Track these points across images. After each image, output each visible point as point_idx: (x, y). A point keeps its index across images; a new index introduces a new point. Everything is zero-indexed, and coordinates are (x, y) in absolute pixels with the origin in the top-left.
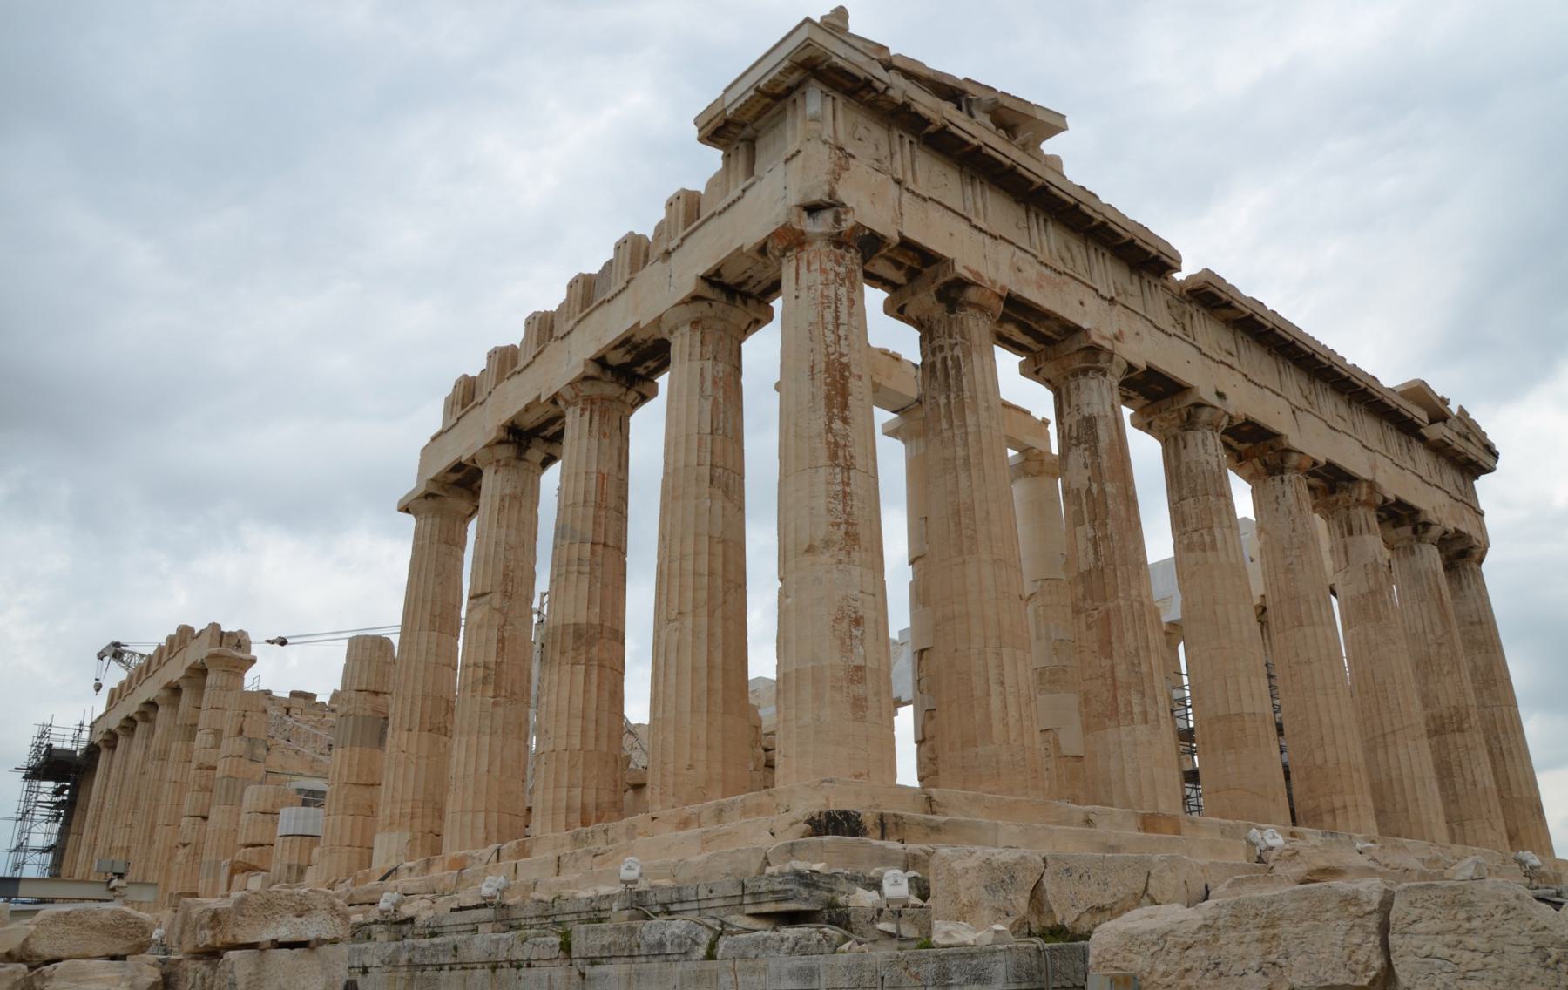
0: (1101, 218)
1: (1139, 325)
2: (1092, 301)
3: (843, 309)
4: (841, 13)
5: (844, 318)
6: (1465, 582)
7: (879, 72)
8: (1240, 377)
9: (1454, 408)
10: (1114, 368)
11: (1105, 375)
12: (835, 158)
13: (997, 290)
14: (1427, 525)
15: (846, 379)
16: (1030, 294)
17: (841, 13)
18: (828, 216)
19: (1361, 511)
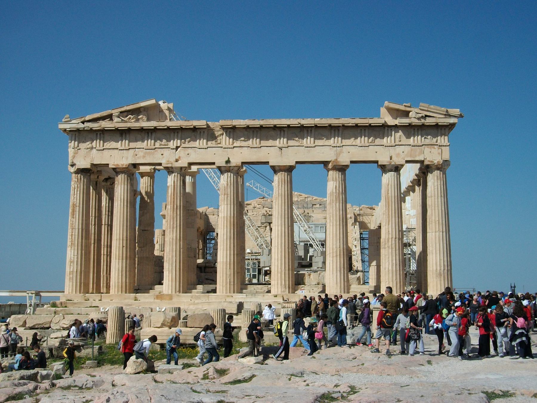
0: (166, 127)
1: (189, 151)
2: (166, 152)
3: (76, 190)
7: (81, 126)
14: (384, 166)
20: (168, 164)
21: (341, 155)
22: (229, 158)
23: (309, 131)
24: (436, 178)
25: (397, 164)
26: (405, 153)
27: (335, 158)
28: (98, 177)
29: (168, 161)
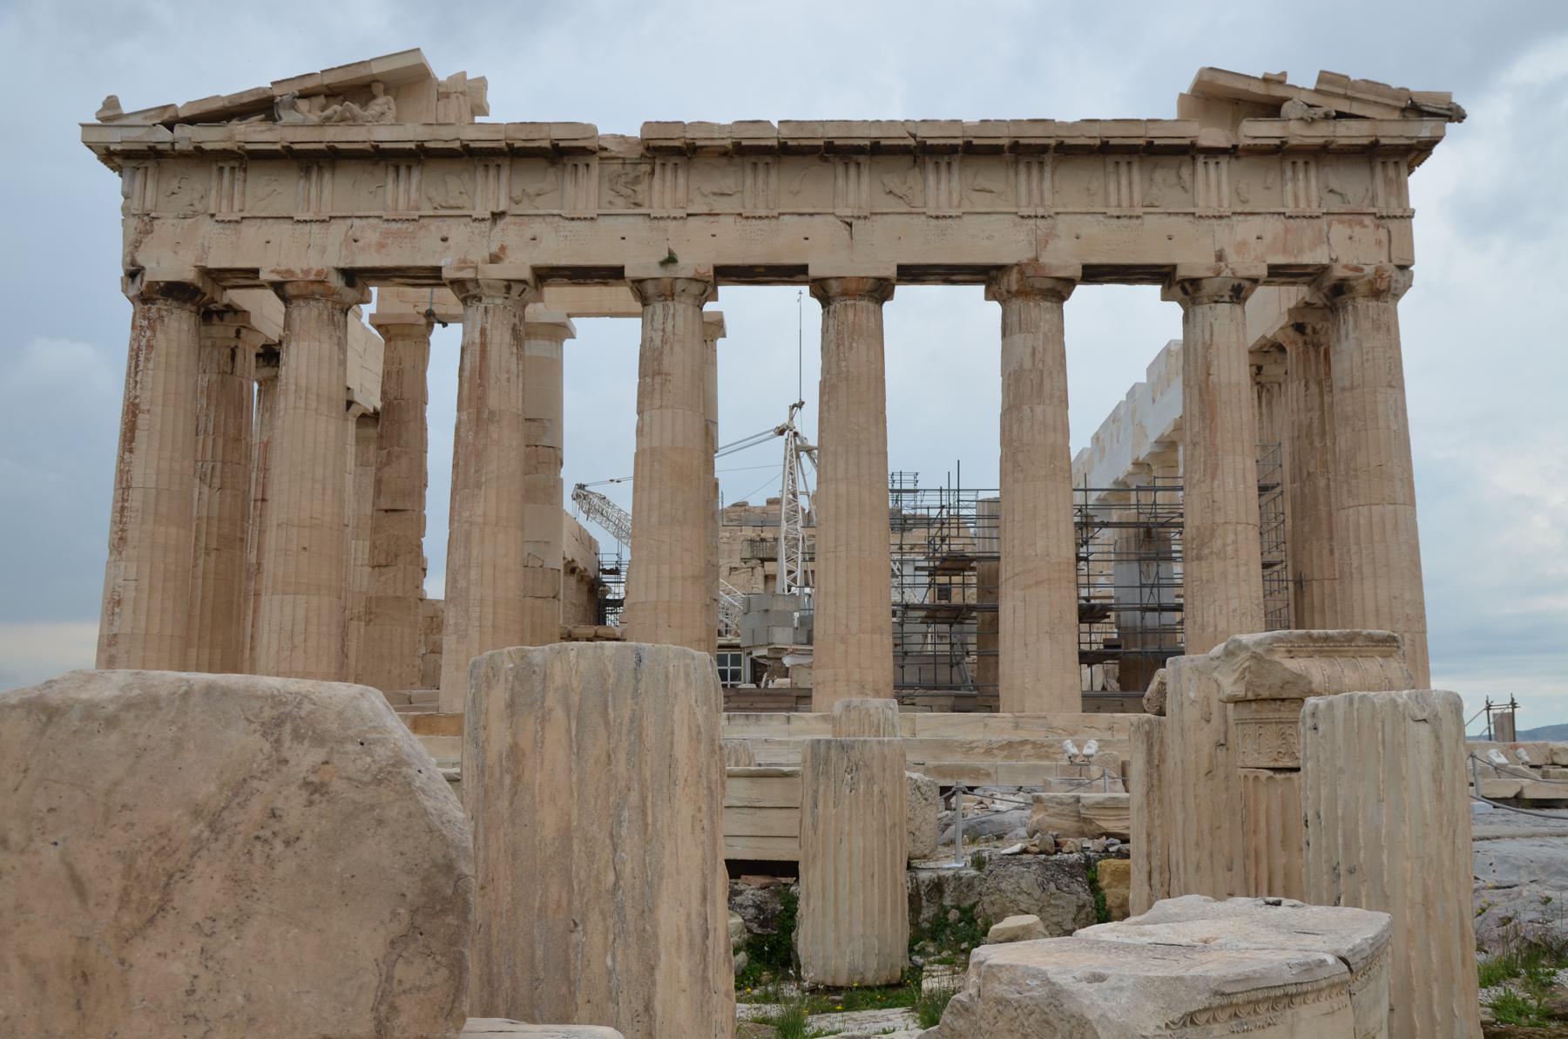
0: (457, 145)
1: (537, 227)
2: (459, 232)
3: (142, 358)
4: (112, 103)
5: (141, 364)
6: (1343, 331)
7: (164, 135)
8: (731, 219)
9: (1303, 78)
10: (486, 291)
11: (480, 300)
12: (141, 226)
13: (312, 277)
14: (1195, 282)
15: (135, 415)
16: (362, 261)
17: (112, 103)
18: (138, 279)
19: (1016, 304)
20: (462, 269)
21: (1050, 247)
22: (670, 252)
23: (943, 167)
24: (1367, 325)
25: (1239, 274)
26: (1268, 238)
27: (1032, 255)
28: (238, 332)
29: (464, 261)
